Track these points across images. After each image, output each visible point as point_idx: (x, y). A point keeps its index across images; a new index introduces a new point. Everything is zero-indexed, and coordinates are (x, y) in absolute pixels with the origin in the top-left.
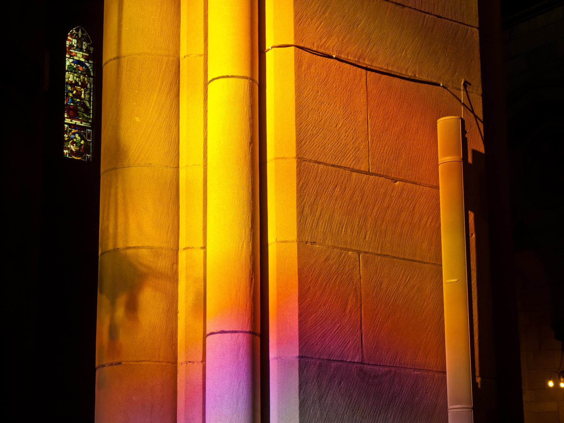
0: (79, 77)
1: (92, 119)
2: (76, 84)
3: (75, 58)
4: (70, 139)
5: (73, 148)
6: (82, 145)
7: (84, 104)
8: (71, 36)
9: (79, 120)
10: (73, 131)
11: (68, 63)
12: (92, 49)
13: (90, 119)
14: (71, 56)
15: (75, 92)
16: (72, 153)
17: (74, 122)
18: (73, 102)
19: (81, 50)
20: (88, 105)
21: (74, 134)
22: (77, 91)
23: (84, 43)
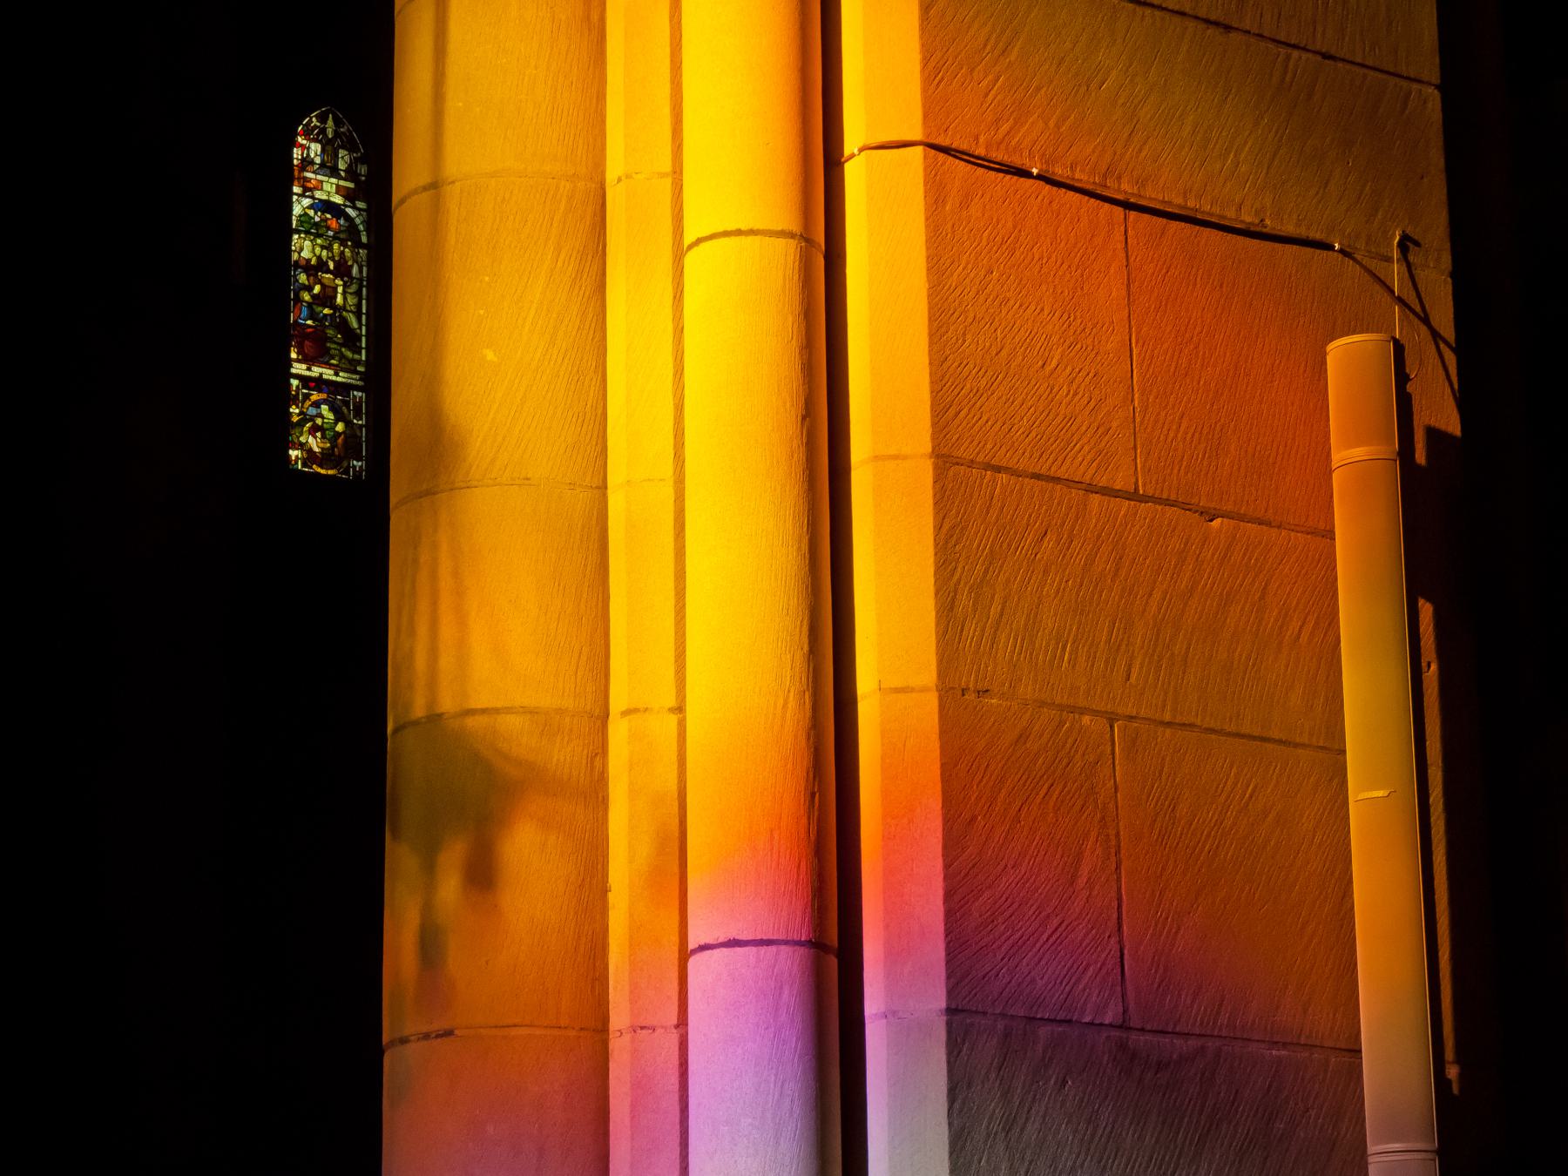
0: (329, 248)
1: (367, 363)
2: (322, 265)
3: (318, 194)
4: (305, 418)
5: (315, 443)
6: (338, 434)
7: (345, 321)
8: (307, 133)
9: (330, 366)
10: (315, 396)
11: (297, 210)
12: (363, 169)
13: (359, 362)
14: (306, 189)
15: (317, 289)
16: (310, 457)
17: (316, 371)
18: (312, 316)
19: (333, 172)
20: (355, 325)
21: (317, 405)
22: (324, 286)
23: (342, 153)
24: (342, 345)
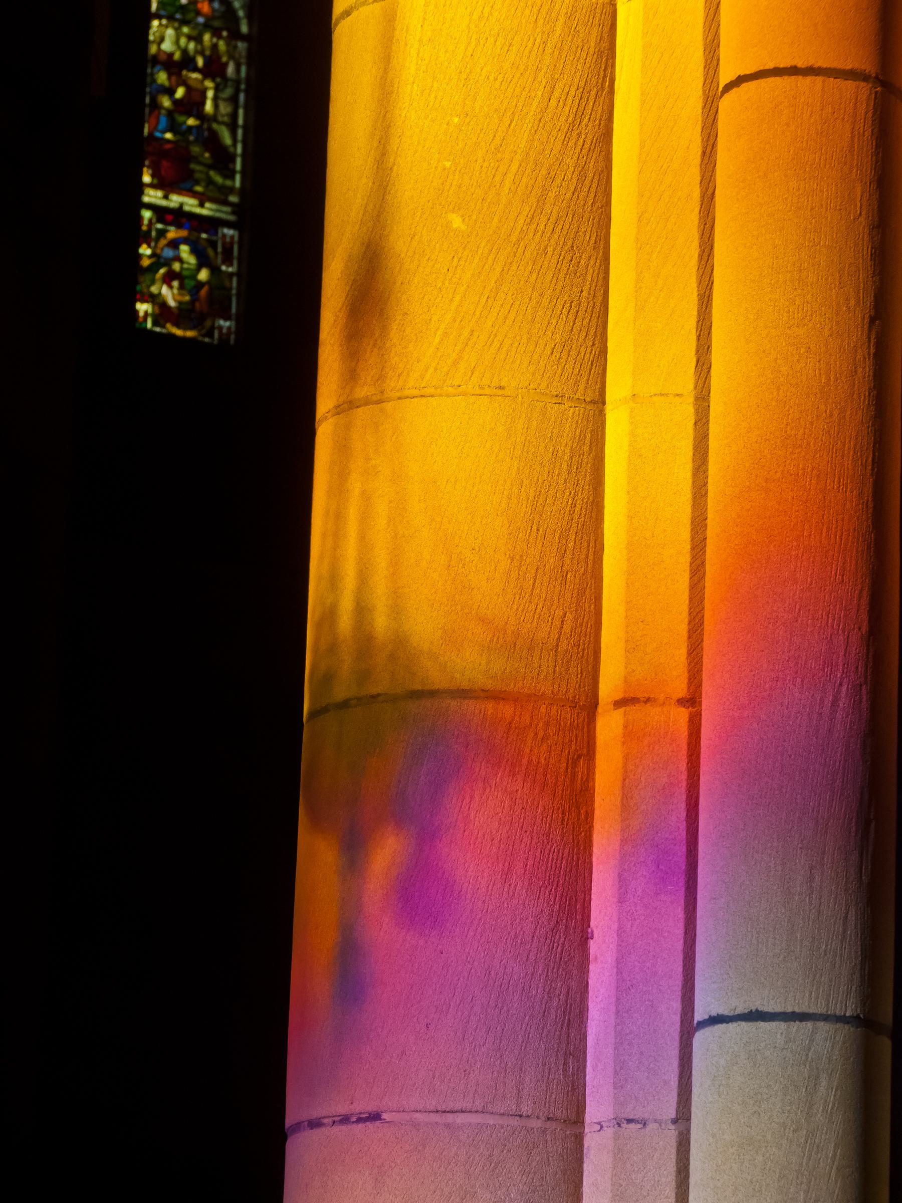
0: (198, 39)
1: (242, 192)
2: (188, 62)
4: (158, 261)
5: (169, 294)
6: (200, 285)
7: (214, 137)
9: (194, 194)
10: (173, 233)
13: (231, 190)
15: (180, 92)
16: (163, 312)
17: (175, 200)
18: (173, 127)
20: (227, 140)
21: (174, 244)
22: (189, 89)
24: (210, 167)
